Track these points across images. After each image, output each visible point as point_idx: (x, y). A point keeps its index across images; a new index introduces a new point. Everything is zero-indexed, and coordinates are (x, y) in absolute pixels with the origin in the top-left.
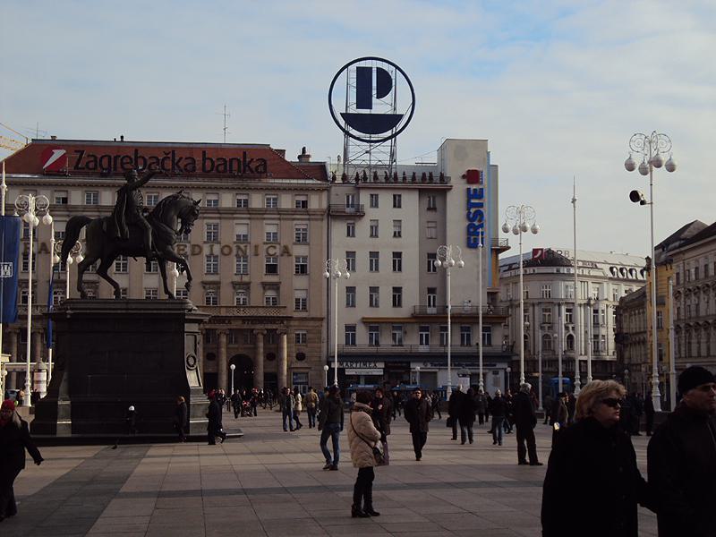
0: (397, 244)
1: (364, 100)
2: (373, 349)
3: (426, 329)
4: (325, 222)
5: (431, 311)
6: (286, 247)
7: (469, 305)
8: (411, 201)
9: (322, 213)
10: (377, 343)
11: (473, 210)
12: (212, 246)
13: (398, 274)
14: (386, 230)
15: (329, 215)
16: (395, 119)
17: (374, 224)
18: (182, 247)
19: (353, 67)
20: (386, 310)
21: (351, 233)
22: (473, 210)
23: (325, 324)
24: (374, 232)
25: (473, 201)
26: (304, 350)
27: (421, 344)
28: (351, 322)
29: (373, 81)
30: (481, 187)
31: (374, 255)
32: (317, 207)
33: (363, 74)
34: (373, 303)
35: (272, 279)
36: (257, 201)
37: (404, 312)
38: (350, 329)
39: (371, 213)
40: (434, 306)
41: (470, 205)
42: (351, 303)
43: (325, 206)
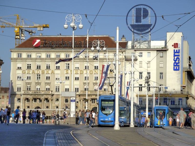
1: (138, 19)
7: (174, 90)
11: (176, 57)
12: (86, 71)
16: (148, 26)
18: (77, 71)
19: (135, 9)
22: (176, 57)
25: (176, 54)
29: (141, 13)
30: (179, 49)
33: (138, 11)
35: (48, 81)
36: (72, 55)
41: (175, 56)
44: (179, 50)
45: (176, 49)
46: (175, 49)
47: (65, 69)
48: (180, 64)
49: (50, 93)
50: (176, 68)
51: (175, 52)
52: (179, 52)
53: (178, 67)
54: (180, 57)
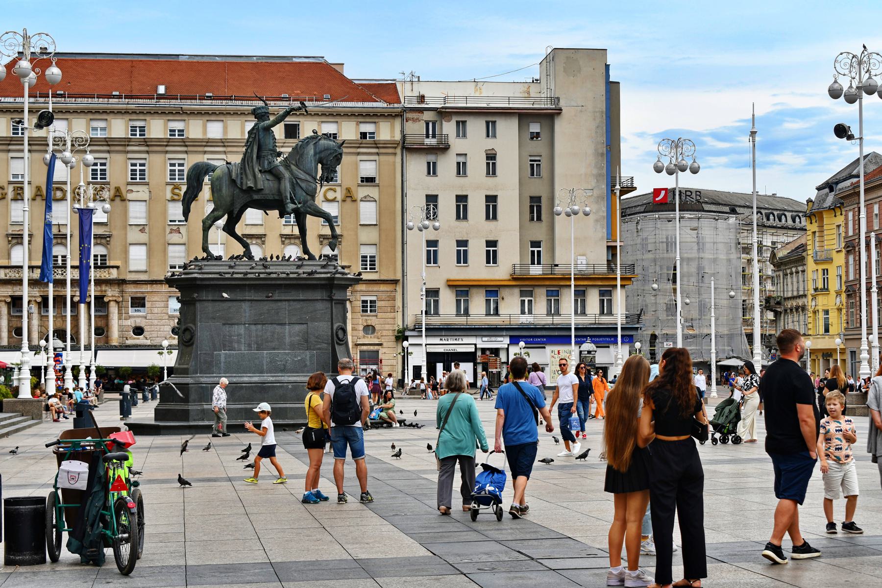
0: (491, 186)
2: (462, 321)
3: (530, 293)
4: (398, 159)
5: (536, 270)
6: (348, 190)
8: (508, 129)
9: (392, 145)
10: (467, 313)
13: (492, 224)
14: (477, 165)
15: (403, 147)
17: (461, 159)
20: (477, 269)
21: (432, 170)
23: (399, 288)
24: (461, 169)
26: (372, 321)
27: (523, 312)
28: (432, 285)
31: (462, 199)
32: (389, 138)
34: (462, 257)
37: (501, 272)
38: (432, 293)
39: (457, 145)
40: (539, 263)
42: (432, 258)
43: (398, 137)
47: (168, 184)
49: (112, 277)
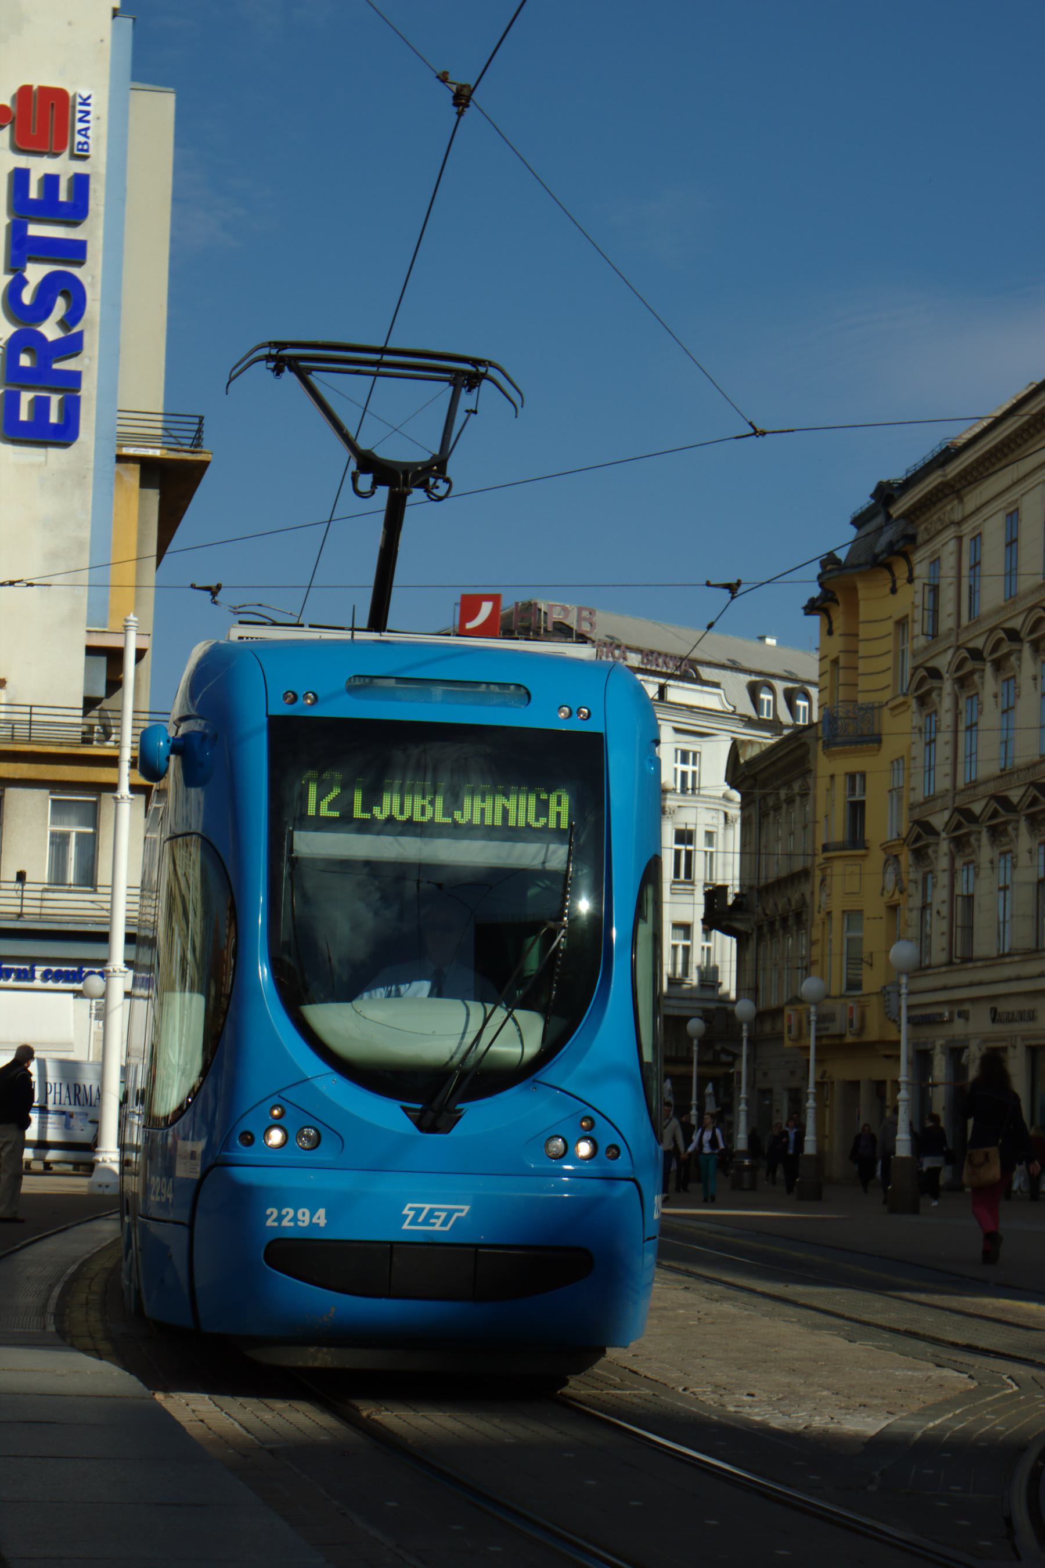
11: (35, 273)
22: (35, 273)
25: (35, 230)
30: (80, 167)
41: (23, 249)
44: (80, 183)
45: (39, 167)
46: (23, 161)
48: (87, 364)
50: (40, 407)
51: (23, 208)
52: (75, 211)
53: (55, 399)
54: (89, 275)
